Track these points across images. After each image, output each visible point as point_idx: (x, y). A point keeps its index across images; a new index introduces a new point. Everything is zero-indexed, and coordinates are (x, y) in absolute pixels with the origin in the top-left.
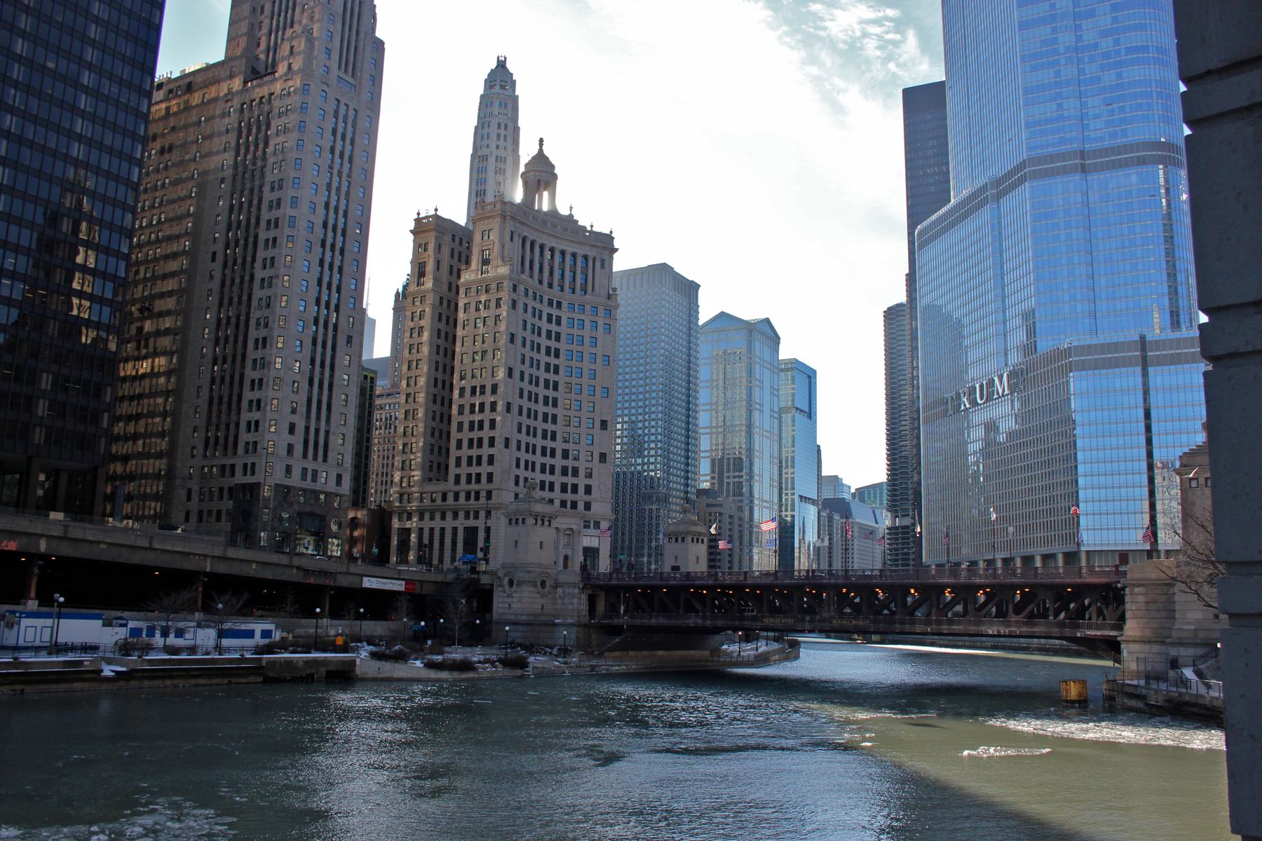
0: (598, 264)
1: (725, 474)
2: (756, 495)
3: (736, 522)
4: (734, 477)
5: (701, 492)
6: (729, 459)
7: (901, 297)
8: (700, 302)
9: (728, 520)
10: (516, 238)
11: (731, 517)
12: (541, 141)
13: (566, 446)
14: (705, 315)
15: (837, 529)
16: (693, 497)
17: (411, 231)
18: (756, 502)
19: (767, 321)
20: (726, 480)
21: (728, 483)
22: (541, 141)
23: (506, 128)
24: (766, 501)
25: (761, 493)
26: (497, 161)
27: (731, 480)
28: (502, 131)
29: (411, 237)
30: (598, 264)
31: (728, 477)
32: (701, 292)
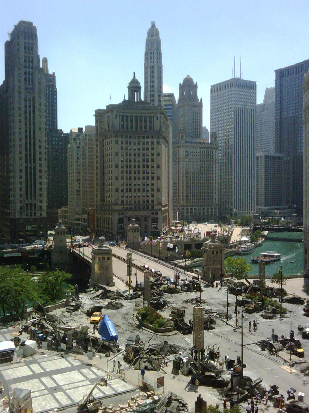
0: (155, 118)
10: (118, 117)
12: (134, 73)
13: (144, 187)
17: (94, 115)
22: (134, 73)
23: (154, 54)
26: (151, 68)
28: (152, 56)
29: (94, 117)
30: (155, 118)
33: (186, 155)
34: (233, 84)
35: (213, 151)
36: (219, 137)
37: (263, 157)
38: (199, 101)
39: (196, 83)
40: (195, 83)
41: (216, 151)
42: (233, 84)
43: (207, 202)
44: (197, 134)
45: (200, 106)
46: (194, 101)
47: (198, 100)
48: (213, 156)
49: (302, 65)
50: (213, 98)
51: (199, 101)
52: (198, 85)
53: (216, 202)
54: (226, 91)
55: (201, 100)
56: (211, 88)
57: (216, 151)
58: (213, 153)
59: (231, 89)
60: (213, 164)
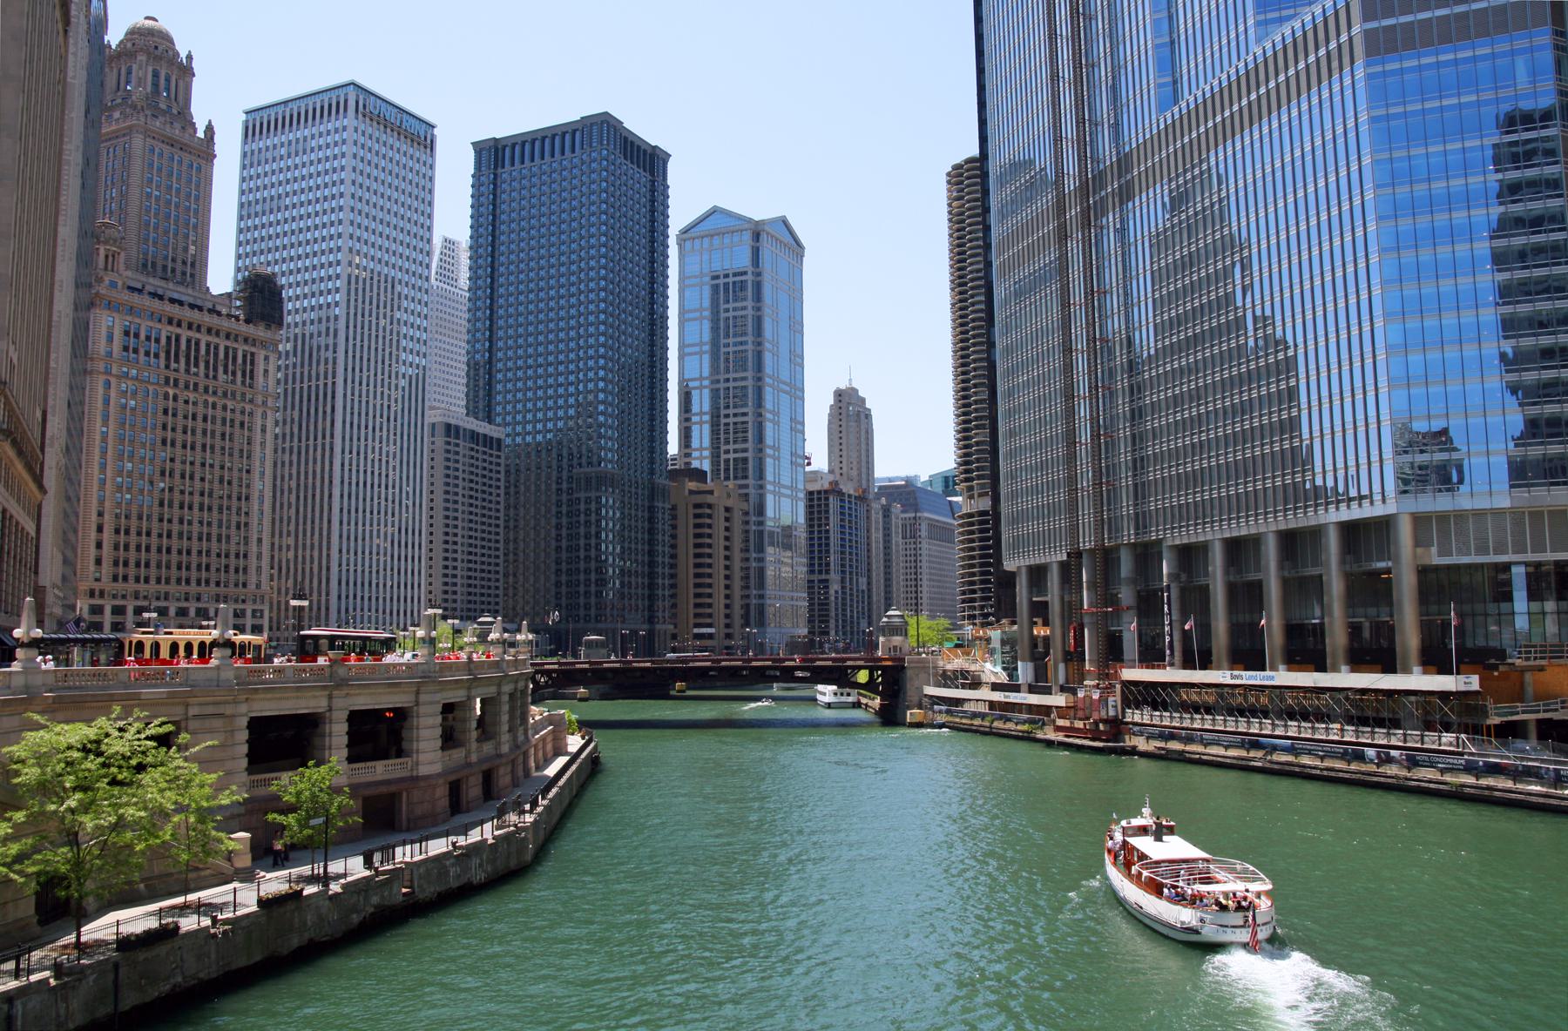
1: (723, 448)
2: (769, 476)
3: (737, 517)
4: (735, 451)
5: (675, 475)
6: (727, 424)
7: (974, 151)
8: (671, 179)
9: (723, 514)
11: (727, 509)
14: (681, 212)
15: (897, 527)
16: (661, 481)
18: (769, 487)
19: (784, 222)
20: (723, 457)
21: (727, 461)
24: (785, 487)
25: (777, 474)
27: (732, 456)
31: (727, 452)
32: (671, 166)
33: (126, 349)
34: (352, 104)
35: (253, 354)
36: (290, 299)
37: (440, 431)
38: (200, 134)
39: (190, 57)
40: (183, 55)
41: (266, 358)
42: (352, 104)
43: (218, 584)
44: (184, 274)
45: (205, 151)
46: (177, 125)
47: (195, 131)
48: (252, 378)
49: (574, 131)
50: (248, 160)
51: (200, 134)
52: (194, 65)
53: (258, 586)
54: (314, 130)
55: (210, 129)
56: (244, 117)
57: (266, 358)
58: (252, 363)
59: (338, 124)
60: (251, 414)
